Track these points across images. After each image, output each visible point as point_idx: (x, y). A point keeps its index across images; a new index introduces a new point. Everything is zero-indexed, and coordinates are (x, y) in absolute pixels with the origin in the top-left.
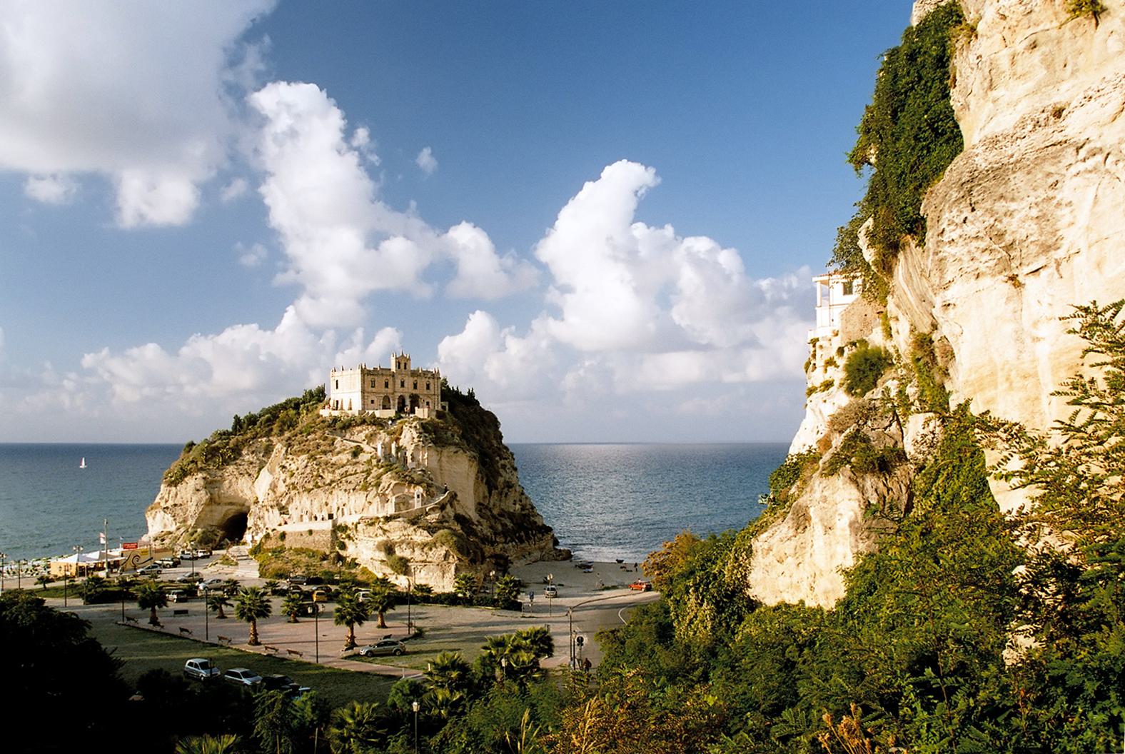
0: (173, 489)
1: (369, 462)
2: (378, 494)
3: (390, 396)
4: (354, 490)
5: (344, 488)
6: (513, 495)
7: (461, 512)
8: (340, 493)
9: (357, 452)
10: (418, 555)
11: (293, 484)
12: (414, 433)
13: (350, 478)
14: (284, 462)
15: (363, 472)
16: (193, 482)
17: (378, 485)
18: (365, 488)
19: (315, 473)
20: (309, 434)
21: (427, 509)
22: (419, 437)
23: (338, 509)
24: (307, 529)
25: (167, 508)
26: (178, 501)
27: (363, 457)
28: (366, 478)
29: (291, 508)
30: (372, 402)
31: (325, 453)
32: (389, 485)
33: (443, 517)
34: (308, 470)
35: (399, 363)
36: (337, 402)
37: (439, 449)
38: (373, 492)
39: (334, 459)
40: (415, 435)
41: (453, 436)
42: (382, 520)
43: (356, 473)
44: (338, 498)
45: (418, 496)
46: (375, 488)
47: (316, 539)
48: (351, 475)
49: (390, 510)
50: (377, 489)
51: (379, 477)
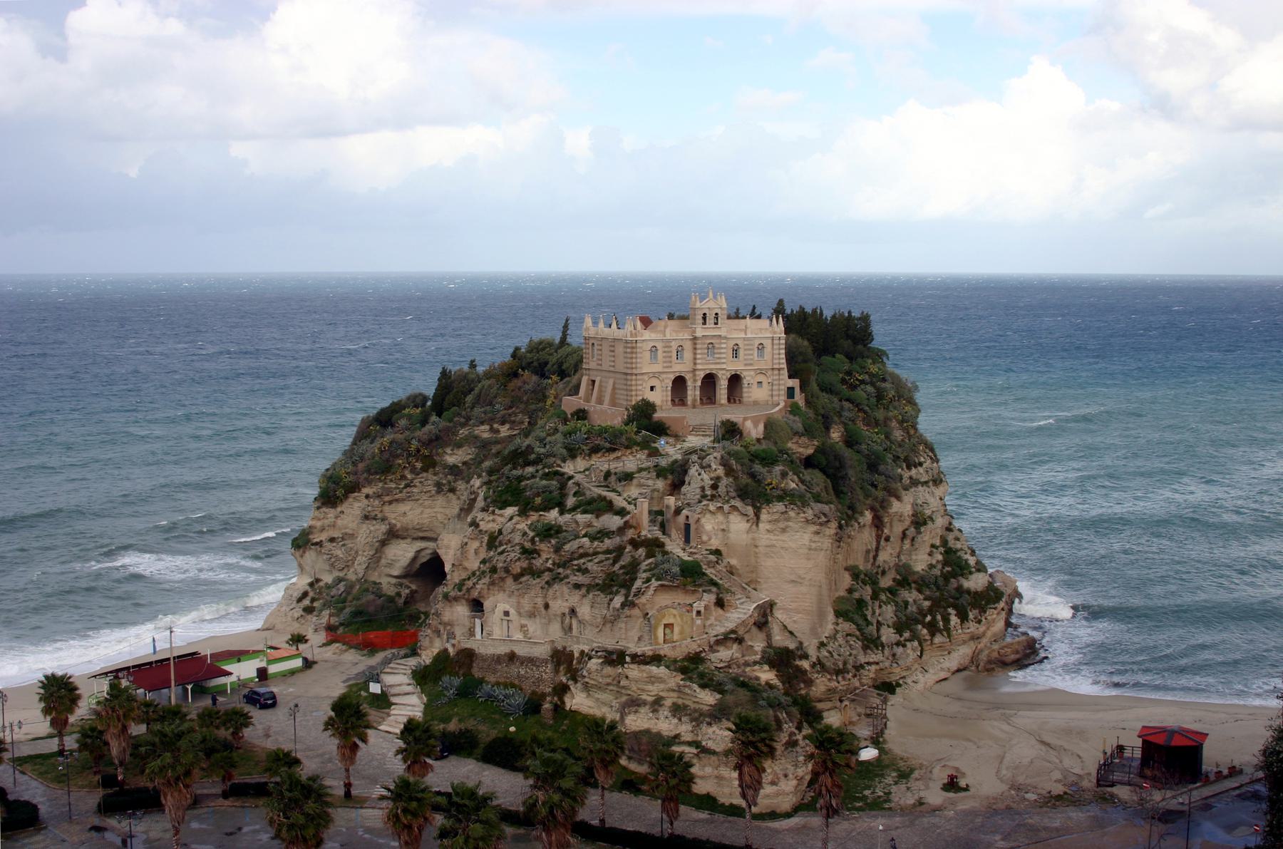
0: (331, 513)
3: (688, 377)
5: (574, 579)
6: (931, 535)
7: (779, 639)
8: (565, 589)
10: (685, 729)
17: (627, 585)
22: (714, 487)
26: (336, 534)
28: (613, 564)
30: (652, 389)
36: (594, 382)
38: (618, 601)
40: (708, 482)
44: (562, 599)
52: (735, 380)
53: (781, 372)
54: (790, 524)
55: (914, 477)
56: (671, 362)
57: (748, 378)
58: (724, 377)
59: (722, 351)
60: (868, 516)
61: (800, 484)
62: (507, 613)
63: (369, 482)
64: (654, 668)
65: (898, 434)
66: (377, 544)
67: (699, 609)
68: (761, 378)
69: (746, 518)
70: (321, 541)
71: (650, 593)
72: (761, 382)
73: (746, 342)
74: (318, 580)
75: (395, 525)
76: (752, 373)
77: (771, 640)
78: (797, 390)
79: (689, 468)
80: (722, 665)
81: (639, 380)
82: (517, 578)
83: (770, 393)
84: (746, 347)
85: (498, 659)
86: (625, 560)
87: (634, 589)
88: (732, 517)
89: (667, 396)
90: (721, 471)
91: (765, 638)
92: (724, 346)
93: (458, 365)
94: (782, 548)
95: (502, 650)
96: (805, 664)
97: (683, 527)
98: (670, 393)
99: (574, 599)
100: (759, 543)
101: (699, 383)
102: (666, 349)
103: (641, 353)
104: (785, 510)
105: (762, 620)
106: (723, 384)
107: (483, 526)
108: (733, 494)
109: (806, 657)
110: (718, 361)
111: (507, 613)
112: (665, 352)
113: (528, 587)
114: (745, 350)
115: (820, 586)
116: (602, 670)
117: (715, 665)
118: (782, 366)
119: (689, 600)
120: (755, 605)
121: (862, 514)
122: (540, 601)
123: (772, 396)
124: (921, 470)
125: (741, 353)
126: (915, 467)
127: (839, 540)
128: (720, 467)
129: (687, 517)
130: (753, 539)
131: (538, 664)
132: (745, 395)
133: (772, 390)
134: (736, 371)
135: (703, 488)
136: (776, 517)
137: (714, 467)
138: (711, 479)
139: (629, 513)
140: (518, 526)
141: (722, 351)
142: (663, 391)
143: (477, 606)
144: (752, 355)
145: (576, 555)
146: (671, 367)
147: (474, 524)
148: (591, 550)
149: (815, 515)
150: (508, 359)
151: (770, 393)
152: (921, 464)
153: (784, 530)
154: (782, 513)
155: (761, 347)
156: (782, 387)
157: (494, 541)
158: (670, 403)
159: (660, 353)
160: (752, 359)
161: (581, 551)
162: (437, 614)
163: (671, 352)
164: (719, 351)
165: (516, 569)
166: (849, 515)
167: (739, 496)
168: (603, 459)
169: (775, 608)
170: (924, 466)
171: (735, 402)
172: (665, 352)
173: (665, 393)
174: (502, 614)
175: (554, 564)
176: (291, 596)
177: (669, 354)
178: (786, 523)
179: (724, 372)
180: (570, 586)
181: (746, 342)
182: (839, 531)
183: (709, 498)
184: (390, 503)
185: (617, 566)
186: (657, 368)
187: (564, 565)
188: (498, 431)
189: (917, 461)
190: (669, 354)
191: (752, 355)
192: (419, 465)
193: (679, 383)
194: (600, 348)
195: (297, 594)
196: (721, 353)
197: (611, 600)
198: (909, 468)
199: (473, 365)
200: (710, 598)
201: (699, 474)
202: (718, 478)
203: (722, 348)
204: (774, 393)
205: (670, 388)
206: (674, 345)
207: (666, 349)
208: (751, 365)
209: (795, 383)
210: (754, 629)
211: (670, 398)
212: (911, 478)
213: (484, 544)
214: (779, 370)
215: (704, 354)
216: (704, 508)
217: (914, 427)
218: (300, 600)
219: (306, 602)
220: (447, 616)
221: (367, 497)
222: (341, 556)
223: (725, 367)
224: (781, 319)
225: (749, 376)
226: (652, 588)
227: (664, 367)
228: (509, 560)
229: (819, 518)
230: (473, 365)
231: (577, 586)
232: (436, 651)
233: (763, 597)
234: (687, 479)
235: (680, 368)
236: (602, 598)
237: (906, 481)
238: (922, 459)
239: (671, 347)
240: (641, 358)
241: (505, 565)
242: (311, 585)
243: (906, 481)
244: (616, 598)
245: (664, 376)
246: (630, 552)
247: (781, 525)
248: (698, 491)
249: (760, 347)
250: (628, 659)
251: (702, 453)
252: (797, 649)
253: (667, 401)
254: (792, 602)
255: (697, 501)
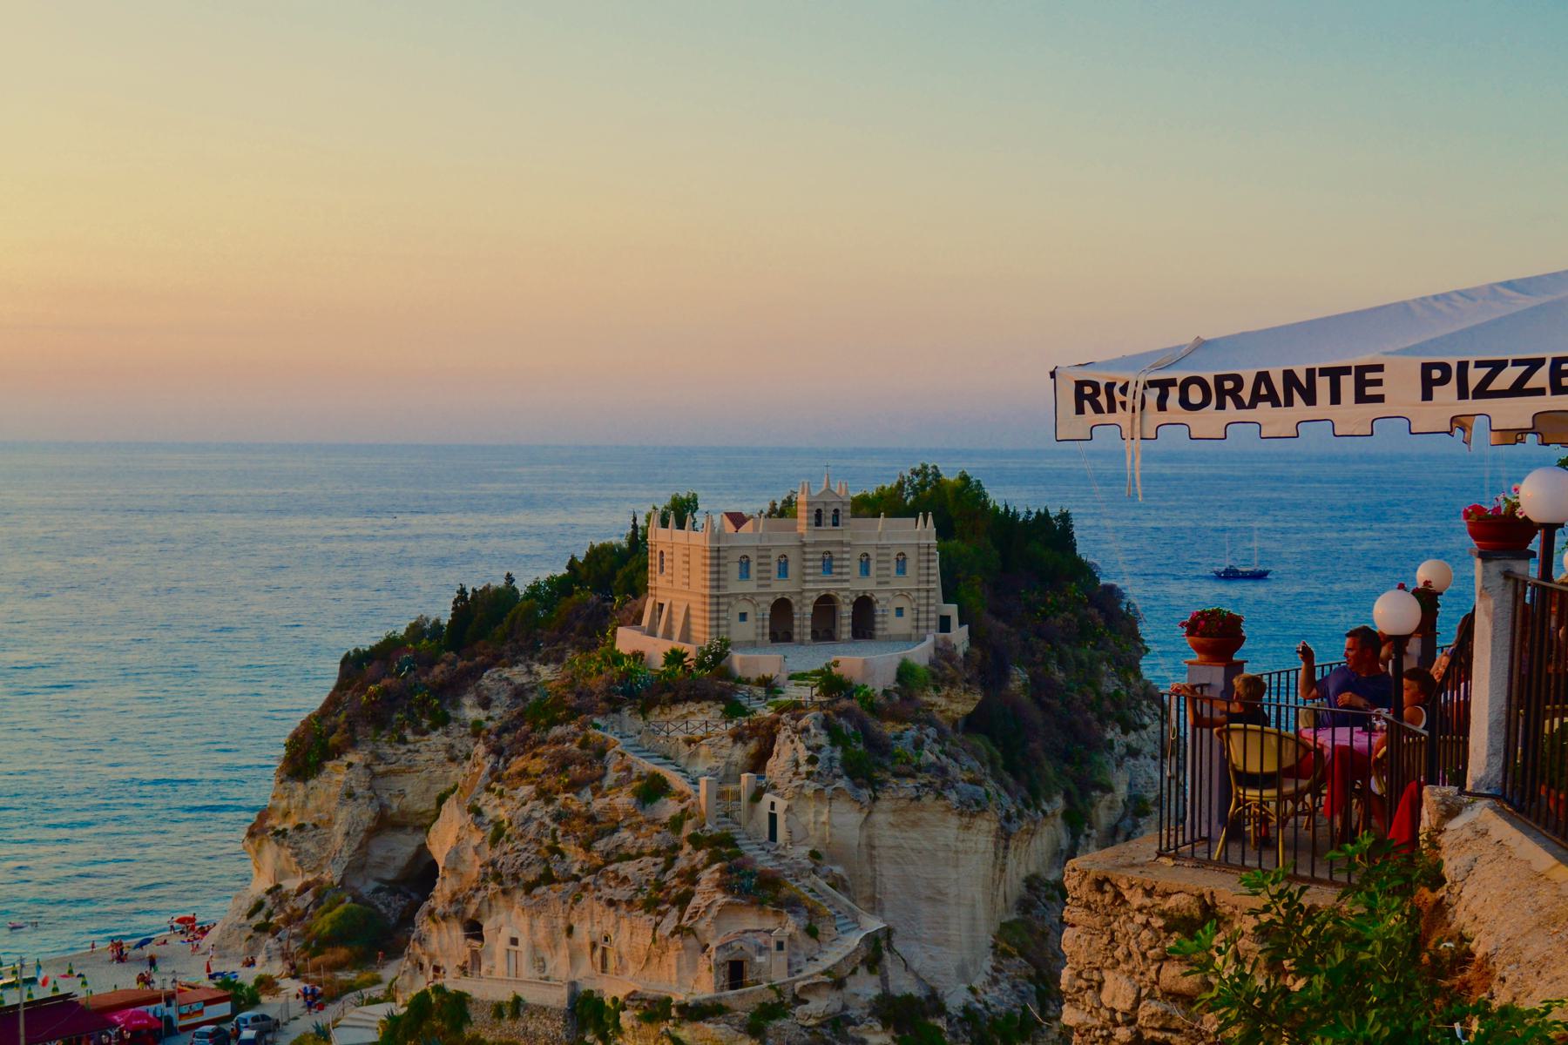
0: (300, 789)
1: (676, 824)
2: (678, 930)
4: (630, 902)
5: (607, 892)
7: (903, 985)
8: (598, 908)
9: (654, 789)
11: (493, 863)
12: (801, 747)
13: (627, 868)
14: (484, 797)
15: (656, 853)
16: (337, 775)
17: (683, 901)
18: (650, 906)
19: (547, 841)
20: (555, 722)
21: (798, 985)
22: (812, 761)
23: (594, 946)
24: (509, 998)
25: (283, 833)
27: (668, 808)
28: (664, 871)
29: (488, 926)
30: (743, 616)
31: (575, 786)
32: (708, 907)
33: (845, 1007)
34: (533, 827)
35: (819, 514)
36: (662, 605)
37: (865, 793)
38: (669, 923)
39: (598, 804)
40: (803, 755)
41: (918, 744)
42: (674, 1012)
43: (640, 855)
44: (593, 922)
45: (780, 946)
46: (675, 912)
47: (531, 1029)
48: (629, 857)
49: (703, 986)
50: (682, 912)
51: (691, 877)
52: (864, 607)
53: (931, 594)
54: (925, 814)
55: (1134, 745)
56: (769, 578)
57: (885, 604)
58: (847, 601)
59: (845, 563)
60: (1059, 803)
61: (943, 757)
62: (514, 941)
63: (352, 744)
64: (710, 1026)
65: (1109, 685)
66: (362, 835)
67: (780, 939)
68: (900, 603)
69: (858, 806)
70: (285, 830)
71: (710, 915)
72: (902, 608)
73: (879, 551)
74: (278, 887)
75: (390, 807)
76: (888, 595)
77: (887, 985)
78: (955, 620)
79: (778, 732)
80: (812, 1022)
81: (723, 604)
82: (529, 888)
83: (915, 624)
84: (881, 558)
85: (498, 1010)
86: (682, 863)
87: (689, 910)
88: (835, 804)
89: (763, 627)
90: (823, 739)
91: (879, 983)
92: (845, 556)
93: (484, 576)
94: (912, 850)
95: (504, 994)
96: (941, 1023)
97: (766, 818)
98: (767, 623)
99: (607, 920)
100: (877, 843)
101: (810, 609)
102: (762, 561)
103: (725, 565)
104: (915, 794)
105: (875, 953)
106: (846, 611)
107: (488, 814)
108: (837, 771)
109: (940, 1010)
110: (839, 577)
111: (514, 941)
112: (759, 564)
113: (545, 903)
114: (878, 562)
115: (973, 906)
116: (640, 1026)
117: (801, 1022)
118: (933, 586)
119: (770, 923)
120: (863, 935)
121: (1049, 800)
122: (561, 923)
123: (917, 627)
124: (1144, 734)
125: (873, 566)
126: (1135, 730)
127: (1007, 836)
128: (823, 732)
129: (773, 805)
130: (869, 837)
131: (553, 1016)
132: (878, 626)
133: (918, 620)
134: (865, 592)
135: (797, 765)
136: (903, 803)
137: (813, 731)
138: (808, 748)
139: (689, 796)
140: (536, 814)
141: (845, 563)
142: (757, 620)
143: (474, 930)
144: (888, 569)
145: (613, 857)
146: (769, 586)
147: (477, 812)
148: (634, 852)
149: (961, 802)
150: (562, 571)
151: (915, 624)
152: (1144, 727)
153: (915, 824)
154: (912, 800)
155: (901, 561)
156: (932, 616)
157: (498, 834)
158: (767, 638)
159: (753, 567)
160: (888, 576)
161: (622, 851)
162: (421, 941)
163: (769, 564)
164: (839, 563)
165: (530, 875)
166: (1033, 796)
167: (848, 774)
168: (662, 717)
169: (894, 938)
170: (1149, 729)
171: (864, 637)
172: (759, 564)
173: (760, 623)
174: (507, 941)
175: (582, 870)
176: (240, 908)
177: (767, 568)
178: (919, 814)
179: (847, 593)
180: (602, 902)
181: (879, 551)
182: (1005, 824)
183: (804, 776)
184: (384, 775)
185: (670, 874)
186: (750, 587)
187: (595, 870)
188: (538, 674)
189: (1138, 721)
190: (767, 568)
191: (888, 569)
192: (426, 723)
193: (782, 609)
194: (671, 557)
195: (247, 905)
196: (842, 567)
197: (657, 924)
198: (1125, 732)
199: (509, 578)
200: (792, 925)
201: (792, 742)
202: (819, 748)
203: (843, 559)
204: (921, 624)
205: (767, 617)
206: (775, 555)
207: (762, 561)
208: (887, 583)
209: (952, 610)
210: (862, 971)
211: (767, 631)
212: (1128, 746)
213: (488, 839)
214: (928, 591)
215: (818, 567)
216: (798, 789)
217: (1136, 670)
218: (251, 915)
219: (259, 918)
220: (433, 944)
221: (350, 765)
222: (313, 851)
223: (849, 586)
224: (930, 518)
225: (884, 599)
226: (714, 910)
227: (759, 586)
228: (520, 861)
229: (969, 807)
230: (509, 578)
231: (611, 903)
232: (414, 993)
233: (873, 924)
234: (776, 748)
235: (780, 587)
236: (644, 920)
237: (1119, 750)
238: (1146, 720)
239: (770, 557)
240: (726, 572)
241: (512, 870)
242: (269, 892)
243: (1119, 750)
244: (665, 921)
245: (758, 599)
246: (689, 854)
247: (911, 816)
248: (790, 764)
249: (901, 558)
250: (674, 1012)
251: (796, 708)
252: (928, 998)
253: (763, 635)
254: (929, 929)
255: (788, 780)
